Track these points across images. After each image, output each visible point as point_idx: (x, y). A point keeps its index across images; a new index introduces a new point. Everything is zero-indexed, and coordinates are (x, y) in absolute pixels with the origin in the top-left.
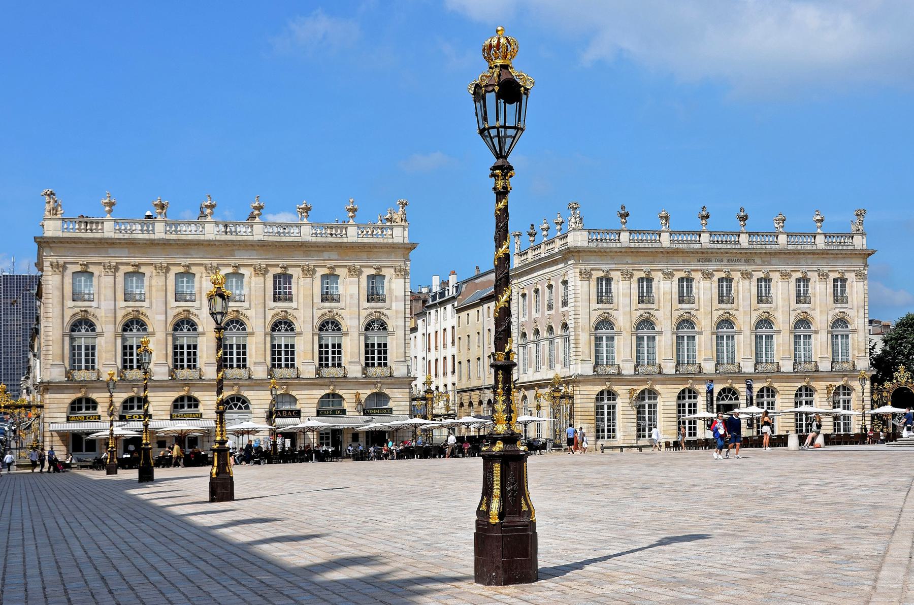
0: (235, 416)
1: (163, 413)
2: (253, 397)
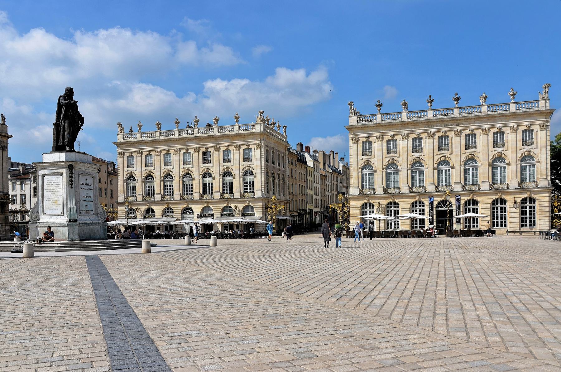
0: (188, 216)
2: (401, 203)
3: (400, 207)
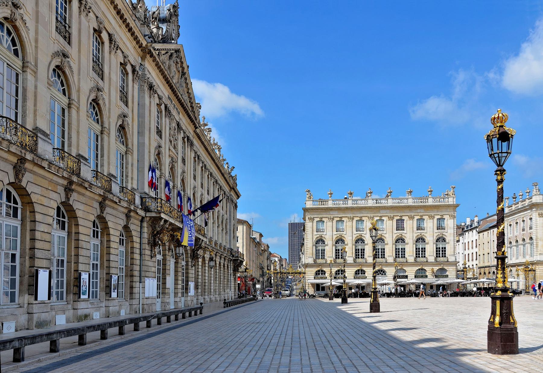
0: (380, 278)
1: (351, 276)
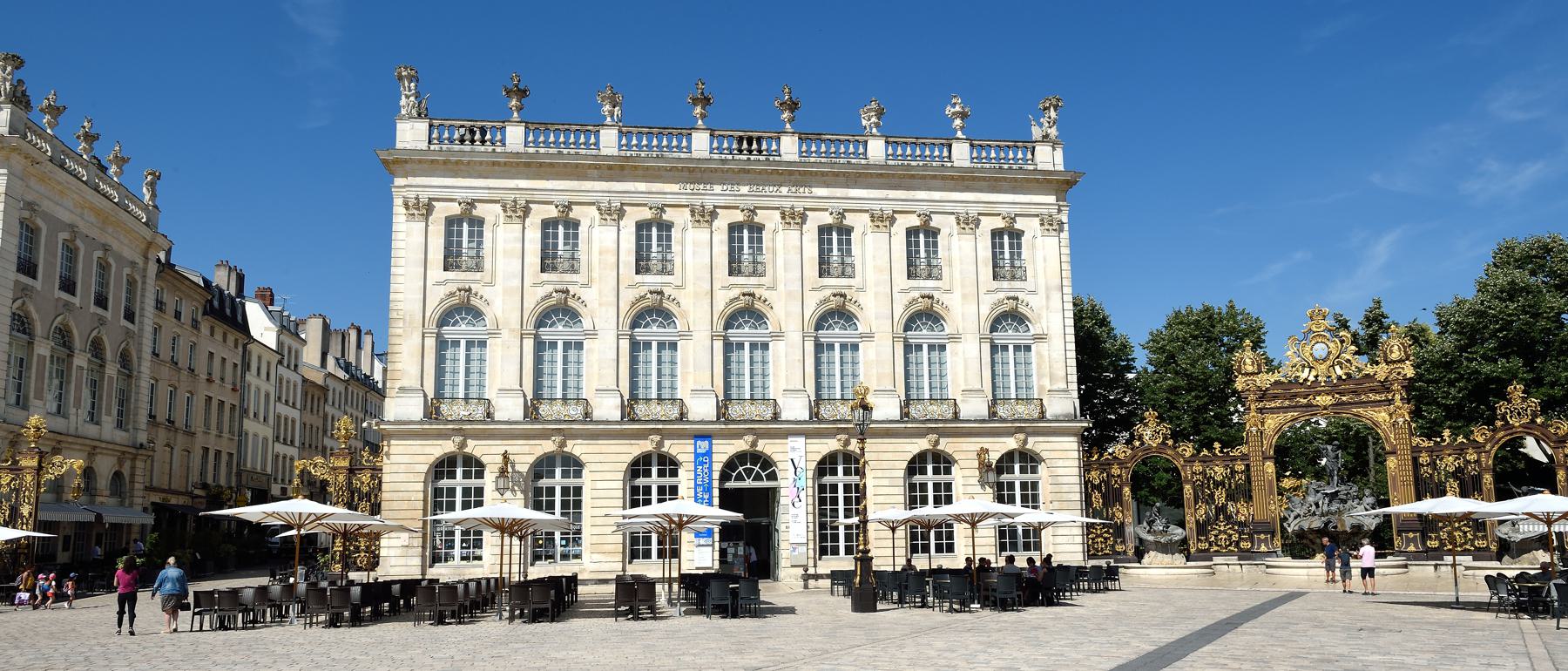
3: (585, 472)
